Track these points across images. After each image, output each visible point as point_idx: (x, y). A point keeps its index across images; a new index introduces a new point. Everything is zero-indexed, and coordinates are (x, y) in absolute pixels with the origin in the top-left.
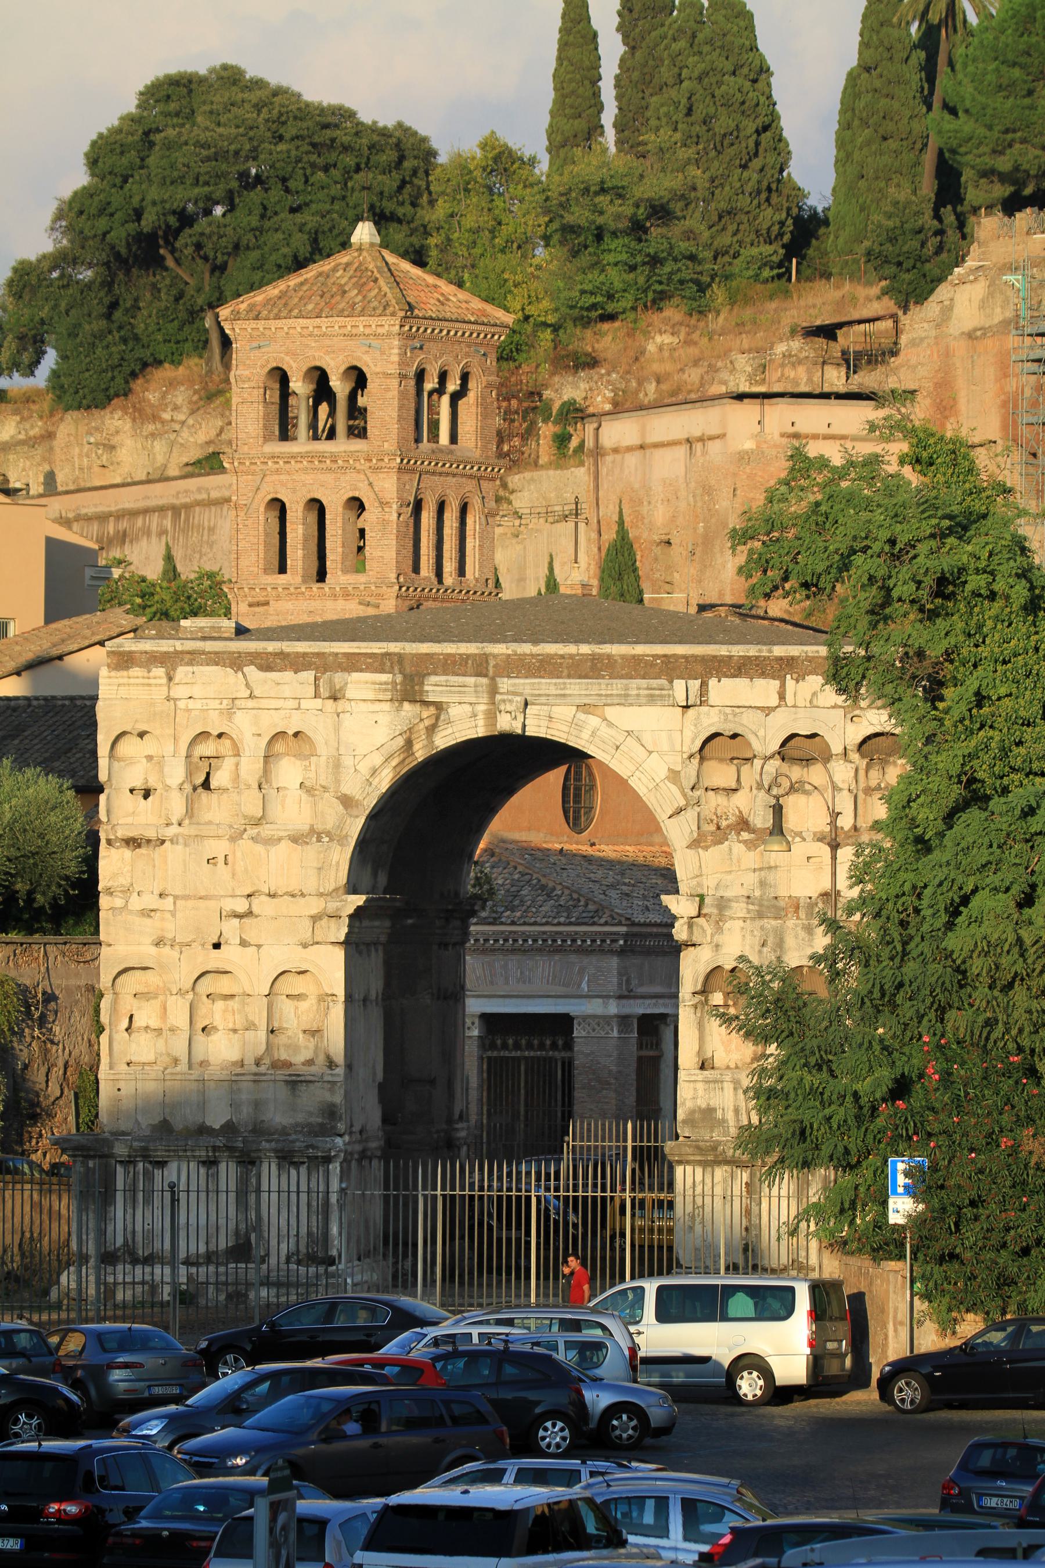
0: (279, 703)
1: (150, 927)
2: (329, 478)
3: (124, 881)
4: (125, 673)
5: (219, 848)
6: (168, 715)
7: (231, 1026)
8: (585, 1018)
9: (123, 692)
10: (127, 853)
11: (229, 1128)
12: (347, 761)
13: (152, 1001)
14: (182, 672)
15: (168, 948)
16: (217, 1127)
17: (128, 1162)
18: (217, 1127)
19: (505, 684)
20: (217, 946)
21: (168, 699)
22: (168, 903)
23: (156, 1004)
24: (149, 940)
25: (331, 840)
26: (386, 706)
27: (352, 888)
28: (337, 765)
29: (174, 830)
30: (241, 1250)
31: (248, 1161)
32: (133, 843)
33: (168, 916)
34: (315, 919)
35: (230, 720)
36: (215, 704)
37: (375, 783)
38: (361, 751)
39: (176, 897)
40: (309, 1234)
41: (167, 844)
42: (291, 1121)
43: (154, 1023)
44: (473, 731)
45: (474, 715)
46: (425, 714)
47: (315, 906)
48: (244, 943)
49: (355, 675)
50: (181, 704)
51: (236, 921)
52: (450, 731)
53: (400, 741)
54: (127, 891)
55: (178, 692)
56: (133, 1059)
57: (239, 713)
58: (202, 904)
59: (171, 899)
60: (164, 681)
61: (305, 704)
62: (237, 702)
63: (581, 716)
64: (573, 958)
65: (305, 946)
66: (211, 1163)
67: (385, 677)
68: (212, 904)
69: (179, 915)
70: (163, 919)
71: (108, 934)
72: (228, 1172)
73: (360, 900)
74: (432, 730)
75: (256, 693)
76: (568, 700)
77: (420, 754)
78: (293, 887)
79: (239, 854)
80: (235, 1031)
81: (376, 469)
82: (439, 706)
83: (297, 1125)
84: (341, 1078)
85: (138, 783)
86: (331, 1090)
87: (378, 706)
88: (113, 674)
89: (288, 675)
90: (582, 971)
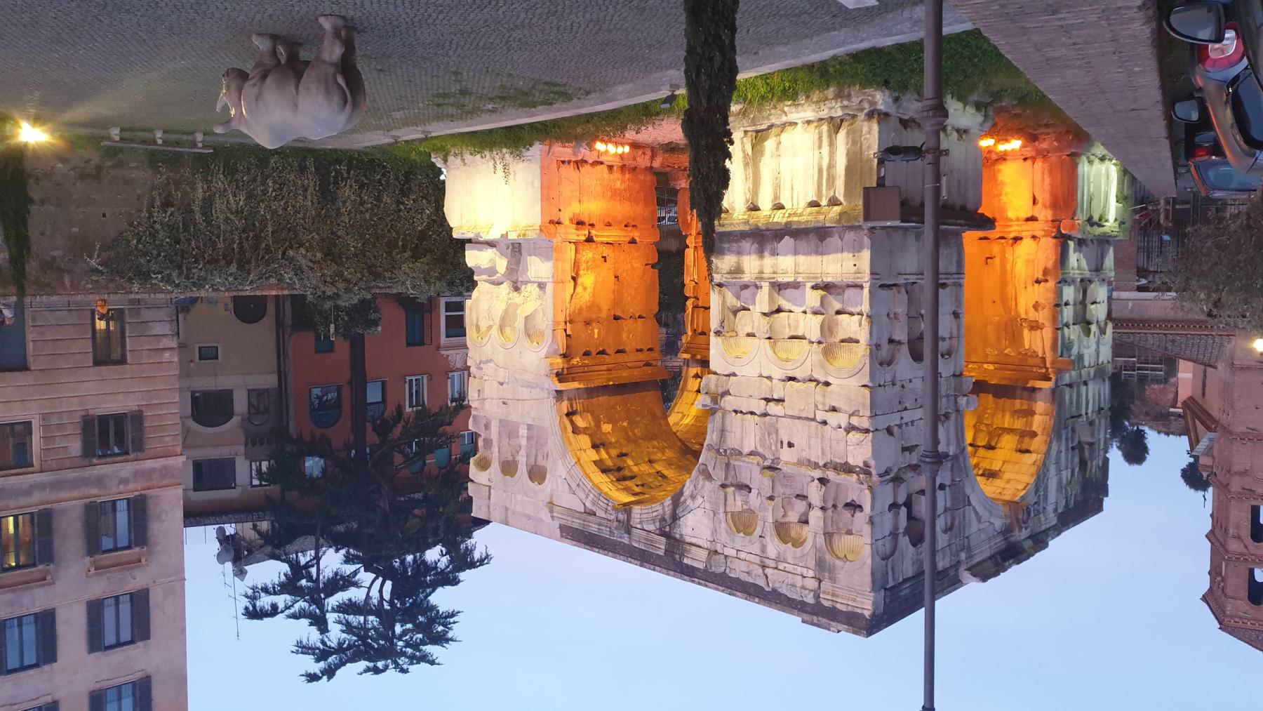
0: (750, 557)
4: (850, 609)
10: (851, 461)
12: (707, 505)
13: (845, 337)
14: (810, 599)
15: (822, 379)
16: (787, 238)
19: (626, 540)
22: (820, 416)
26: (688, 539)
29: (817, 474)
32: (847, 469)
33: (820, 407)
34: (727, 393)
36: (790, 568)
37: (692, 488)
38: (701, 511)
39: (814, 420)
41: (821, 464)
45: (641, 523)
46: (667, 529)
48: (769, 378)
49: (701, 566)
50: (811, 574)
51: (776, 397)
54: (851, 428)
55: (812, 584)
56: (858, 290)
57: (773, 557)
58: (796, 413)
59: (819, 419)
61: (733, 553)
64: (1137, 317)
65: (734, 375)
67: (685, 561)
70: (824, 404)
74: (663, 520)
75: (760, 570)
76: (598, 520)
81: (1241, 554)
82: (663, 534)
83: (737, 241)
85: (858, 514)
87: (694, 541)
88: (859, 611)
90: (1132, 311)
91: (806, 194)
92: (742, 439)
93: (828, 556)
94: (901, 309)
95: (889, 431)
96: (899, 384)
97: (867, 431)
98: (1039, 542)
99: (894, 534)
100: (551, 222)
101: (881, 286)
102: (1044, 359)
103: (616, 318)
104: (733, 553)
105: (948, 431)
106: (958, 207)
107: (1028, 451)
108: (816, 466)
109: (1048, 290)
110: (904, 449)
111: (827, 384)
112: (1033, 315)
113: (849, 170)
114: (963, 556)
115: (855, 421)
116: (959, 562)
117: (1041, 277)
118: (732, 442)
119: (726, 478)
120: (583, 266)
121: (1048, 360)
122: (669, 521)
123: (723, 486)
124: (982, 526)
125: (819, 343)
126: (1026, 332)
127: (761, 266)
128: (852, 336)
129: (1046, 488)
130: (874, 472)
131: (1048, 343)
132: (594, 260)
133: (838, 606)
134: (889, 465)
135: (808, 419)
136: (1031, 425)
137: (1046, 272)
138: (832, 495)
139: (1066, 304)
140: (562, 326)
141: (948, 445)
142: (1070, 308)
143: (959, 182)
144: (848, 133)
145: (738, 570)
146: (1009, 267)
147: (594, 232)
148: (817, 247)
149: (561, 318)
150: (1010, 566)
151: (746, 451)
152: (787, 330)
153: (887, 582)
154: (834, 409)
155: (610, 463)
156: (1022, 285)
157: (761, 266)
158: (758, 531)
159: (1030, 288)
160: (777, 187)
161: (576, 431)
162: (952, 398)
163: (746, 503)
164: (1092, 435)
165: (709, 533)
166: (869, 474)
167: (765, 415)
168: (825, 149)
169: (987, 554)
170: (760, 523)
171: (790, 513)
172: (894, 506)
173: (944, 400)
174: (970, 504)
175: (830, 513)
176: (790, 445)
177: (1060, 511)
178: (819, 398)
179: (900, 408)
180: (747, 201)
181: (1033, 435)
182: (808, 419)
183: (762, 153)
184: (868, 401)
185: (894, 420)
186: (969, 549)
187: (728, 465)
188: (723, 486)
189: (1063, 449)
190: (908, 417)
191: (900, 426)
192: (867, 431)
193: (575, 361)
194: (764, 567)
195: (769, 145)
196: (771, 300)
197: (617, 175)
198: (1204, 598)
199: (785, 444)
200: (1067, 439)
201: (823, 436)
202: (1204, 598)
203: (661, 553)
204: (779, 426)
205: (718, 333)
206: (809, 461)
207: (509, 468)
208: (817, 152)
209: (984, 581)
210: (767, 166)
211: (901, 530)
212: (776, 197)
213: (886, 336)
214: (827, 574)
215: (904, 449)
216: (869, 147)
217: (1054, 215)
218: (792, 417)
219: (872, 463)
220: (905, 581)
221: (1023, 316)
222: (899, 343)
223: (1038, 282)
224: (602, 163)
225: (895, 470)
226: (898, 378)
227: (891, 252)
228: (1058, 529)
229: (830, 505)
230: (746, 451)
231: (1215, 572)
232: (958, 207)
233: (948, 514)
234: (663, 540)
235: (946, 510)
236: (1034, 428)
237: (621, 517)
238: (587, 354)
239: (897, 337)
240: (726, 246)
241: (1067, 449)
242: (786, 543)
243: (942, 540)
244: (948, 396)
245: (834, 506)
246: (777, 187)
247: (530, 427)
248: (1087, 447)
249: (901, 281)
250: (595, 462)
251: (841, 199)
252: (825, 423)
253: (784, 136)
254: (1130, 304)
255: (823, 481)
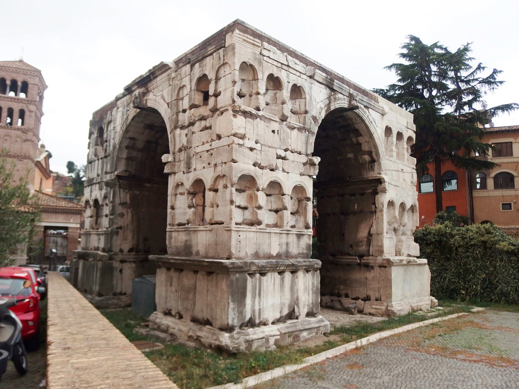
0: (294, 72)
1: (253, 156)
2: (16, 104)
3: (242, 131)
5: (275, 126)
6: (260, 61)
7: (270, 208)
8: (71, 228)
9: (244, 43)
11: (279, 256)
12: (314, 103)
13: (243, 194)
14: (266, 45)
16: (275, 255)
17: (252, 275)
18: (275, 255)
20: (272, 170)
21: (260, 53)
23: (244, 195)
24: (252, 163)
25: (309, 133)
26: (323, 86)
27: (314, 154)
28: (311, 103)
29: (260, 113)
30: (291, 315)
31: (293, 272)
32: (245, 114)
33: (259, 152)
34: (305, 164)
35: (280, 72)
36: (276, 63)
40: (312, 303)
41: (258, 119)
42: (298, 252)
43: (243, 204)
44: (343, 104)
46: (333, 93)
47: (304, 159)
48: (283, 170)
52: (338, 102)
53: (327, 102)
54: (243, 137)
55: (265, 52)
59: (259, 145)
60: (260, 45)
62: (283, 66)
63: (365, 109)
65: (302, 175)
66: (281, 273)
68: (274, 151)
69: (263, 153)
70: (257, 154)
71: (236, 156)
72: (288, 275)
73: (319, 159)
75: (290, 64)
77: (332, 108)
78: (299, 150)
79: (282, 131)
80: (270, 210)
81: (29, 104)
83: (299, 254)
84: (312, 234)
86: (309, 239)
88: (241, 33)
89: (297, 61)
90: (71, 218)
91: (267, 281)
92: (297, 138)
93: (256, 67)
94: (208, 210)
95: (219, 137)
96: (212, 165)
97: (235, 135)
98: (129, 90)
99: (217, 79)
100: (385, 267)
101: (223, 223)
102: (120, 187)
103: (343, 214)
104: (302, 76)
105: (180, 142)
106: (172, 270)
107: (131, 139)
108: (261, 117)
109: (116, 224)
110: (210, 128)
111: (254, 165)
112: (125, 212)
113: (244, 295)
114: (173, 75)
115: (241, 142)
116: (176, 71)
117: (119, 230)
118: (303, 136)
119: (305, 117)
120: (365, 243)
121: (118, 186)
122: (332, 98)
123: (306, 112)
124: (161, 93)
125: (258, 190)
126: (128, 202)
127: (287, 238)
128: (239, 194)
129: (122, 119)
130: (231, 112)
131: (117, 196)
132: (358, 246)
133: (252, 38)
134: (221, 118)
135: (265, 145)
136: (128, 153)
137: (117, 233)
138: (253, 101)
139: (107, 216)
140: (378, 210)
141: (180, 134)
142: (104, 214)
143: (171, 285)
144: (245, 318)
145: (300, 66)
146: (136, 237)
147: (358, 261)
148: (259, 248)
149: (378, 214)
150: (146, 73)
151: (296, 131)
152: (272, 200)
153: (224, 51)
154: (251, 149)
155: (352, 135)
156: (129, 227)
157: (287, 238)
158: (290, 86)
159: (126, 224)
160: (282, 285)
161: (370, 153)
162: (177, 160)
163: (293, 104)
164: (96, 149)
165: (313, 88)
166: (234, 111)
167: (286, 150)
168: (257, 308)
169: (158, 79)
170: (289, 90)
171: (273, 95)
172: (217, 95)
173: (182, 159)
174: (168, 104)
175: (254, 91)
176: (273, 131)
177: (115, 108)
178: (259, 157)
179: (212, 151)
180: (297, 277)
181: (127, 147)
182: (265, 145)
183: (290, 306)
184: (234, 152)
185: (216, 144)
186: (169, 79)
187: (304, 124)
188: (306, 112)
189: (112, 141)
190: (207, 147)
191: (212, 140)
192: (235, 135)
193: (370, 191)
194: (288, 66)
195: (286, 312)
196: (281, 218)
197: (343, 292)
198: (47, 87)
199: (276, 132)
200: (110, 146)
201: (257, 135)
202: (47, 87)
203: (336, 81)
204: (279, 144)
205: (308, 199)
206: (264, 121)
207: (400, 135)
208: (261, 306)
209: (162, 62)
210: (287, 298)
211: (213, 82)
212: (282, 280)
213: (219, 193)
214: (257, 57)
215: (210, 128)
216: (234, 309)
217: (112, 264)
218: (272, 147)
219: (232, 117)
220: (211, 54)
221: (129, 210)
222: (210, 190)
223: (121, 228)
224: (353, 299)
225: (216, 115)
226: (213, 168)
227: (216, 244)
228: (118, 99)
229: (254, 96)
230: (296, 131)
231: (41, 98)
232: (172, 270)
233: (181, 96)
234: (335, 88)
235: (182, 99)
236: (126, 151)
237: (354, 102)
238: (363, 194)
239: (212, 193)
240: (305, 251)
241: (109, 141)
242: (277, 77)
243: (186, 81)
244: (180, 161)
245: (251, 96)
246: (282, 285)
247: (392, 156)
248: (99, 143)
249: (209, 227)
250: (361, 135)
251: (248, 277)
252: (256, 143)
253: (278, 316)
254: (72, 221)
255: (258, 109)
